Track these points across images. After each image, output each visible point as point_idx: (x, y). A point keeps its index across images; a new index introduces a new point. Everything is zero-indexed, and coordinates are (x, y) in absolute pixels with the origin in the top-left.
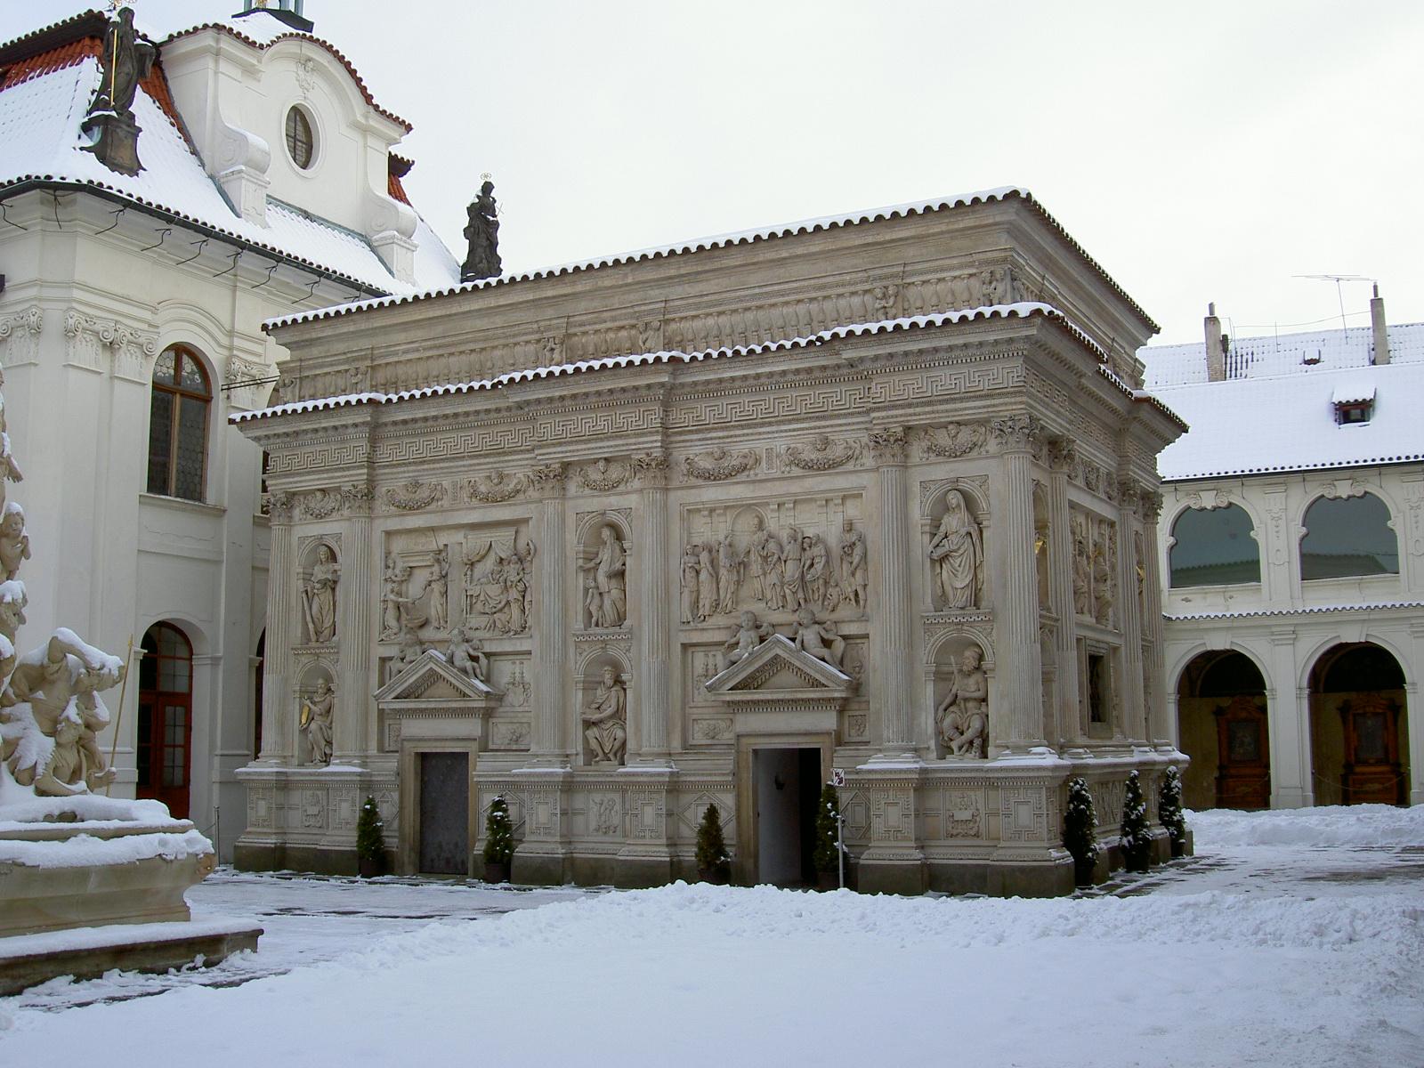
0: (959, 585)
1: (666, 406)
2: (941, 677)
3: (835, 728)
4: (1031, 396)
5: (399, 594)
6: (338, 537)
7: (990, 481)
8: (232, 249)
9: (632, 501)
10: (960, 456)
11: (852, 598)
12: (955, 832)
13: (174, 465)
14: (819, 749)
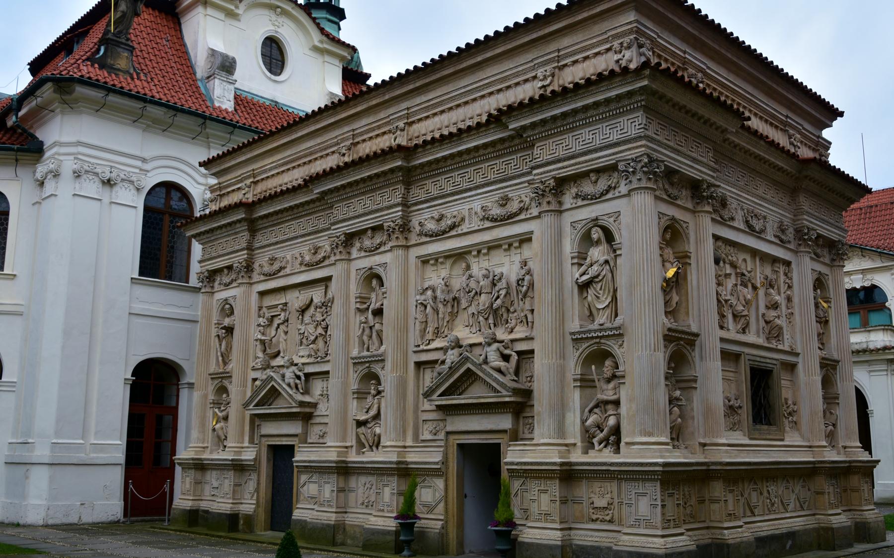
0: (601, 306)
1: (408, 184)
2: (585, 383)
3: (510, 426)
4: (647, 137)
5: (263, 334)
6: (234, 297)
7: (621, 217)
8: (201, 121)
9: (387, 258)
10: (599, 198)
11: (524, 320)
12: (594, 517)
13: (159, 258)
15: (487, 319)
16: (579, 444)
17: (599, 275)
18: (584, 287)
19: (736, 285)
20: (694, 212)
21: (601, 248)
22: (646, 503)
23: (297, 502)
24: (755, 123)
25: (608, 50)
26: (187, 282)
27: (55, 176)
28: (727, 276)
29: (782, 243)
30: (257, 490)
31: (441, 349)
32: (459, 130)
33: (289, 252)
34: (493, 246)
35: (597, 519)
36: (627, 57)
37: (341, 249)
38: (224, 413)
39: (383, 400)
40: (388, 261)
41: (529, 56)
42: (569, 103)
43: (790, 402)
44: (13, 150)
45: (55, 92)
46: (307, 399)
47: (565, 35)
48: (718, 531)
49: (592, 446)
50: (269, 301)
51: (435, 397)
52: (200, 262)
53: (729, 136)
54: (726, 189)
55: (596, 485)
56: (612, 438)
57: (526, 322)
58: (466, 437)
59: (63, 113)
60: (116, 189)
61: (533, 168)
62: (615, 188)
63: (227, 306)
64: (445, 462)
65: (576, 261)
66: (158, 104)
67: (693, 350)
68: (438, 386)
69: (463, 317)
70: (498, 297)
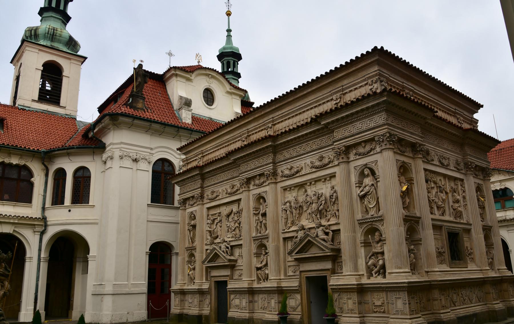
1: (275, 153)
2: (367, 244)
3: (331, 267)
5: (210, 228)
6: (196, 211)
8: (177, 129)
9: (267, 188)
12: (375, 310)
13: (160, 194)
14: (326, 276)
15: (316, 215)
16: (365, 274)
17: (369, 191)
18: (362, 198)
19: (437, 192)
20: (413, 158)
21: (369, 178)
22: (400, 302)
23: (230, 308)
24: (440, 114)
25: (366, 84)
26: (173, 205)
27: (111, 159)
28: (433, 188)
29: (458, 171)
30: (210, 303)
31: (295, 231)
32: (298, 126)
33: (221, 188)
34: (317, 180)
35: (377, 311)
36: (375, 87)
37: (245, 185)
38: (193, 266)
39: (268, 257)
40: (268, 190)
41: (329, 90)
42: (349, 110)
43: (469, 248)
44: (92, 148)
45: (110, 120)
46: (232, 258)
47: (345, 79)
48: (438, 315)
49: (372, 275)
50: (212, 212)
51: (293, 254)
52: (179, 195)
53: (428, 121)
54: (429, 146)
55: (375, 295)
56: (381, 271)
57: (335, 215)
58: (310, 273)
59: (114, 130)
60: (139, 163)
61: (334, 142)
62: (374, 149)
63: (193, 215)
64: (300, 286)
65: (357, 185)
66: (157, 122)
67: (419, 225)
68: (295, 249)
69: (305, 215)
70: (321, 205)
